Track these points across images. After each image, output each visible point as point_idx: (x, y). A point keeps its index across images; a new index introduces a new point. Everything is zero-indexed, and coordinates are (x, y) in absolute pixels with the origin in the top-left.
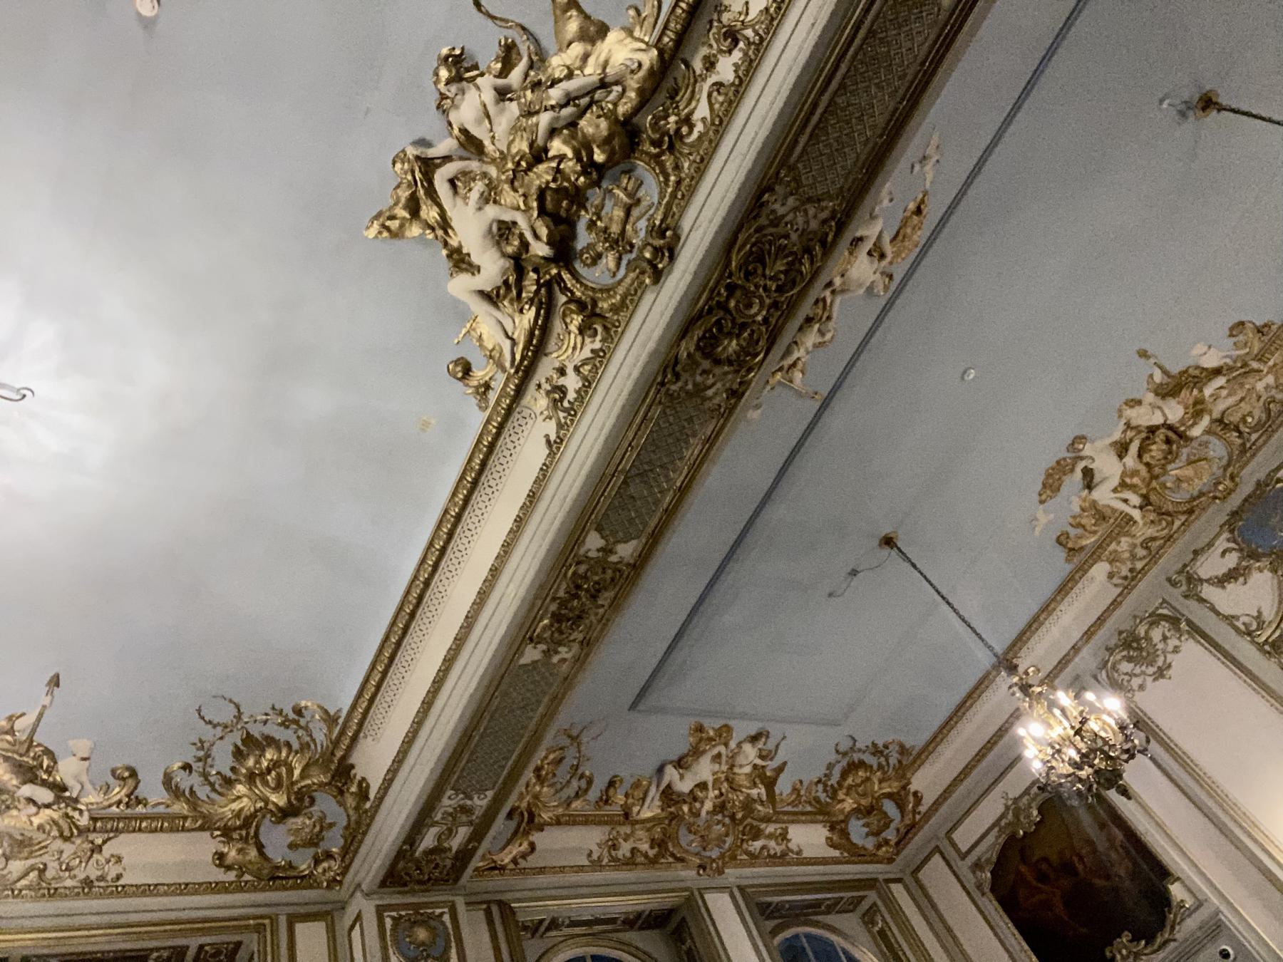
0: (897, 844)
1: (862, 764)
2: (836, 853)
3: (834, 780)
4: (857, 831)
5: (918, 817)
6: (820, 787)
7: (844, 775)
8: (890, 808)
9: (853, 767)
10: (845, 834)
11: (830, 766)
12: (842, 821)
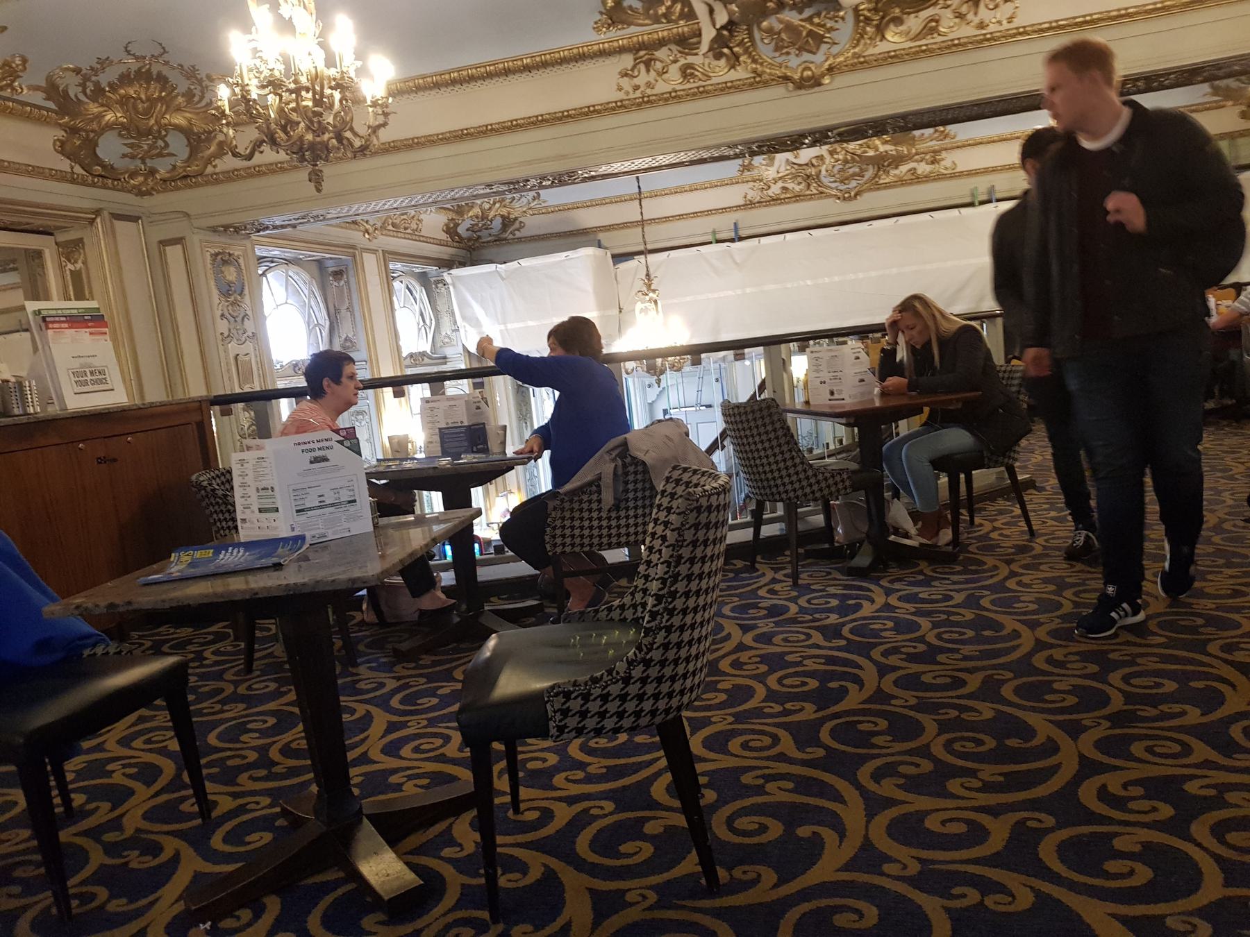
0: (165, 181)
1: (162, 79)
2: (64, 165)
3: (104, 79)
4: (111, 149)
5: (209, 169)
6: (78, 79)
7: (125, 79)
8: (178, 145)
9: (144, 76)
10: (91, 145)
11: (104, 63)
12: (93, 131)
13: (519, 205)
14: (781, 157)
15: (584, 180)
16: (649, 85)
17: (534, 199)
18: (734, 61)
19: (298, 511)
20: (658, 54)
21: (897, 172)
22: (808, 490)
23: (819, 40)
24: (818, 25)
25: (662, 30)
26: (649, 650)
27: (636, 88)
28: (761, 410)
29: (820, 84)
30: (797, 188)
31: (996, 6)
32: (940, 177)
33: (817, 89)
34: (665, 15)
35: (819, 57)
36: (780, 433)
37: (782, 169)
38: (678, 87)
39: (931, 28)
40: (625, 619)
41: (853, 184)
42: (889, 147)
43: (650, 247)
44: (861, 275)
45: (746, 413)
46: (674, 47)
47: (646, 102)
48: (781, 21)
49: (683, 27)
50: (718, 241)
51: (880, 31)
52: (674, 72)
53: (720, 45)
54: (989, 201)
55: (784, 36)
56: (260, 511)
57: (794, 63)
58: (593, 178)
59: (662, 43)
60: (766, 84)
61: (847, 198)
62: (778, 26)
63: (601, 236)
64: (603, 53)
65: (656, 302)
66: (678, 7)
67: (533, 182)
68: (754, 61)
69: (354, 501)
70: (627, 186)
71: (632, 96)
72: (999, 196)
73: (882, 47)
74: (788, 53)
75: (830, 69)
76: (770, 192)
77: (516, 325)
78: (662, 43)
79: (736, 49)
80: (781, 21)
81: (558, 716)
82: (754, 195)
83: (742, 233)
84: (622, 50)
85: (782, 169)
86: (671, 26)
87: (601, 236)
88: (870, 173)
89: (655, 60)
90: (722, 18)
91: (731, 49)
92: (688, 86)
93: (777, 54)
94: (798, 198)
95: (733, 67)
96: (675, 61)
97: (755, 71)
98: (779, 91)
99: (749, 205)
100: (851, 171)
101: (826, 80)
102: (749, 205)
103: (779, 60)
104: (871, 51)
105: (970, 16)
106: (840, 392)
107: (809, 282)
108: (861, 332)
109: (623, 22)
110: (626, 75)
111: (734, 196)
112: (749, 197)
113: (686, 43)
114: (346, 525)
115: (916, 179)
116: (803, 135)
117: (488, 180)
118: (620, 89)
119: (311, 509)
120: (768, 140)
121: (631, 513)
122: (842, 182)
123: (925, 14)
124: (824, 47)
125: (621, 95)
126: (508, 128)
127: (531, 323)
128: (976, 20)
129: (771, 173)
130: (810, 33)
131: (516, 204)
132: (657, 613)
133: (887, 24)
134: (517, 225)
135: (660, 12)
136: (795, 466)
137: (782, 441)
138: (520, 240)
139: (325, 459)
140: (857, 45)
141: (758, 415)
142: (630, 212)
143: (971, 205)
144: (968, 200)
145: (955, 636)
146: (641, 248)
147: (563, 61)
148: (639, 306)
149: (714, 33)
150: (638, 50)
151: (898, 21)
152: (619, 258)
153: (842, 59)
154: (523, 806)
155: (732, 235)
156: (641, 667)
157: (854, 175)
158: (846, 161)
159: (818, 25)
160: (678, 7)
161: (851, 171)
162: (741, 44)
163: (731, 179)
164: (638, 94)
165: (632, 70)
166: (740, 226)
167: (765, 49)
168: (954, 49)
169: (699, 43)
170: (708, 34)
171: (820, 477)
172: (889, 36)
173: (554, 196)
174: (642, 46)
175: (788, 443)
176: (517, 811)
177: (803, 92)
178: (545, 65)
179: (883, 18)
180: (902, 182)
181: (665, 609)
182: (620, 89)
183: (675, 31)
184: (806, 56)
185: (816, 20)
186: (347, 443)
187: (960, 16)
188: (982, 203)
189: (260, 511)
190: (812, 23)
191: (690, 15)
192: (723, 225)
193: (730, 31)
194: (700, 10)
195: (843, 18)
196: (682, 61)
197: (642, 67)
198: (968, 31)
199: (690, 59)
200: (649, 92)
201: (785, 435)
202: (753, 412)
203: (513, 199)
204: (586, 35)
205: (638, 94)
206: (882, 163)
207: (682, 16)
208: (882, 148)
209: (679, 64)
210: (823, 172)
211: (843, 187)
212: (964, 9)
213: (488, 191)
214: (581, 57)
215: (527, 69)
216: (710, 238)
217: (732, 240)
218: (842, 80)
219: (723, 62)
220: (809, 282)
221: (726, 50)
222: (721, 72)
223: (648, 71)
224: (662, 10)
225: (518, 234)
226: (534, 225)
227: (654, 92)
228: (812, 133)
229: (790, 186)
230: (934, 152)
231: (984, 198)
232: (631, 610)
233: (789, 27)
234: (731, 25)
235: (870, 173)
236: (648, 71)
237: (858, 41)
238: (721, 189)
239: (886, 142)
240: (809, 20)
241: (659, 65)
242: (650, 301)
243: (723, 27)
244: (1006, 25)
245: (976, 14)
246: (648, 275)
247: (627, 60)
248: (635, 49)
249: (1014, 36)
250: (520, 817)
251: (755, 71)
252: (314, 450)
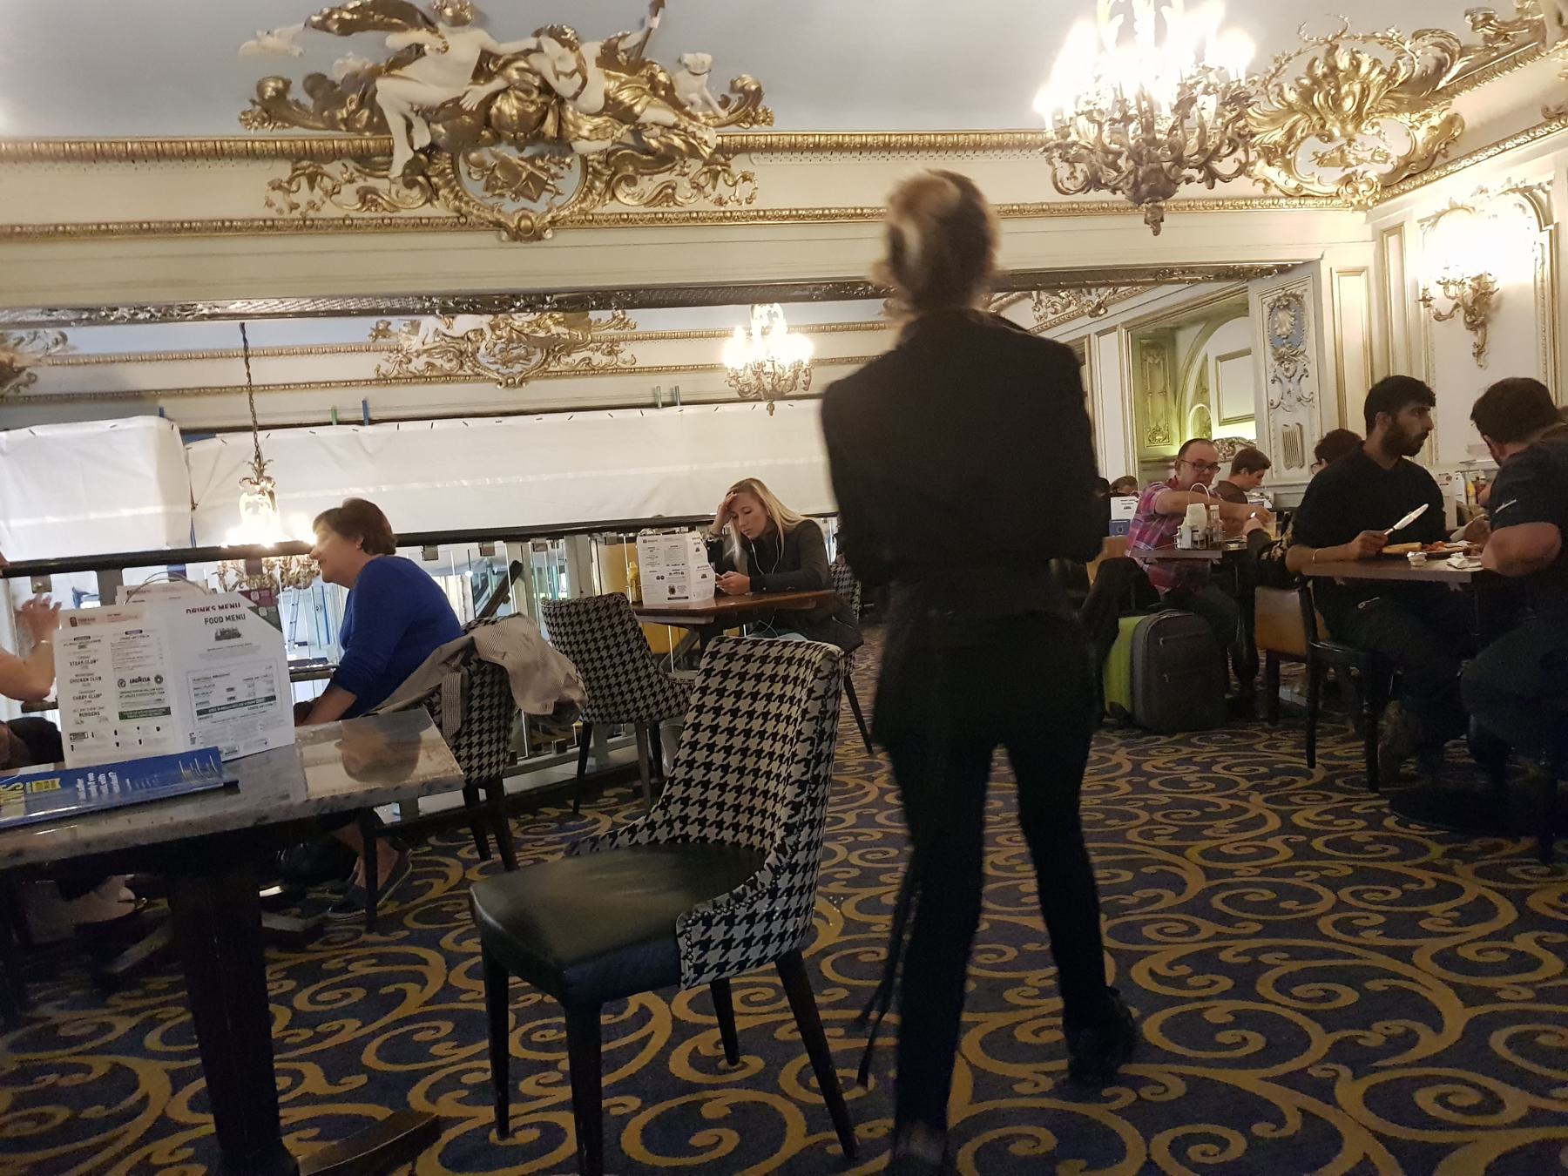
13: (29, 351)
14: (429, 323)
15: (202, 317)
16: (312, 205)
17: (57, 343)
18: (432, 193)
19: (200, 713)
20: (326, 168)
21: (569, 360)
22: (663, 706)
23: (541, 186)
24: (541, 168)
25: (340, 139)
26: (795, 852)
27: (294, 207)
28: (607, 607)
29: (540, 238)
30: (447, 366)
31: (735, 184)
32: (617, 371)
33: (535, 243)
34: (345, 121)
35: (540, 206)
36: (631, 636)
37: (429, 340)
38: (354, 215)
39: (666, 195)
40: (657, 840)
41: (518, 368)
42: (562, 330)
43: (260, 422)
44: (530, 478)
45: (578, 613)
46: (351, 164)
47: (306, 227)
48: (496, 156)
49: (369, 141)
50: (339, 423)
51: (611, 190)
52: (349, 194)
53: (416, 172)
54: (673, 404)
55: (498, 173)
56: (123, 716)
57: (510, 209)
58: (213, 317)
59: (336, 155)
60: (471, 227)
61: (511, 384)
62: (491, 162)
63: (162, 403)
64: (251, 155)
65: (271, 494)
66: (365, 113)
67: (124, 312)
68: (456, 197)
69: (274, 698)
70: (224, 335)
71: (286, 215)
72: (683, 399)
73: (611, 207)
74: (502, 196)
75: (553, 222)
76: (411, 367)
77: (25, 522)
78: (336, 155)
79: (435, 180)
80: (496, 156)
81: (696, 951)
82: (388, 368)
83: (374, 415)
84: (279, 155)
85: (429, 340)
86: (351, 135)
87: (162, 403)
88: (537, 357)
89: (323, 175)
90: (422, 138)
91: (428, 178)
92: (367, 215)
93: (488, 194)
94: (448, 377)
95: (429, 200)
96: (351, 181)
97: (458, 210)
98: (489, 238)
99: (383, 380)
100: (515, 352)
101: (548, 234)
102: (383, 380)
103: (491, 202)
104: (598, 210)
105: (708, 189)
106: (683, 588)
107: (465, 483)
108: (692, 523)
109: (284, 120)
110: (280, 187)
111: (364, 366)
112: (383, 370)
113: (369, 162)
114: (261, 735)
115: (591, 370)
116: (515, 296)
117: (52, 300)
118: (270, 204)
119: (219, 709)
120: (467, 296)
121: (475, 739)
122: (504, 364)
124: (546, 196)
125: (271, 213)
126: (134, 231)
127: (50, 519)
128: (715, 195)
129: (415, 343)
130: (531, 176)
131: (26, 348)
132: (800, 804)
133: (619, 181)
134: (24, 376)
135: (339, 116)
136: (648, 676)
137: (634, 645)
138: (29, 400)
139: (235, 634)
140: (584, 199)
141: (603, 613)
142: (234, 373)
143: (654, 406)
144: (650, 400)
145: (880, 856)
146: (250, 422)
147: (190, 155)
148: (245, 498)
149: (410, 155)
150: (300, 159)
151: (631, 180)
152: (190, 435)
153: (567, 212)
154: (512, 1124)
155: (361, 416)
156: (787, 875)
157: (519, 358)
158: (510, 340)
159: (541, 168)
160: (365, 113)
161: (515, 352)
162: (441, 174)
163: (360, 344)
164: (296, 214)
165: (290, 182)
166: (371, 405)
167: (473, 185)
168: (692, 223)
169: (391, 163)
170: (402, 155)
171: (677, 689)
172: (620, 195)
173: (87, 340)
174: (311, 155)
175: (640, 648)
176: (504, 1132)
177: (518, 244)
178: (160, 156)
179: (614, 174)
180: (574, 373)
181: (809, 798)
182: (270, 204)
183: (357, 143)
184: (524, 202)
185: (539, 162)
186: (263, 611)
187: (698, 187)
188: (665, 405)
189: (123, 716)
190: (533, 165)
191: (381, 127)
192: (350, 402)
193: (428, 156)
194: (396, 124)
195: (569, 166)
196: (360, 183)
197: (304, 182)
198: (704, 205)
199: (371, 182)
200: (312, 214)
201: (637, 639)
202: (587, 612)
203: (22, 340)
204: (229, 128)
205: (296, 214)
206: (553, 348)
207: (369, 126)
208: (555, 330)
209: (355, 186)
210: (482, 350)
211: (503, 370)
212: (702, 180)
213: (45, 318)
214: (217, 154)
215: (132, 157)
216: (329, 418)
217: (361, 423)
219: (416, 192)
220: (465, 483)
221: (420, 179)
222: (415, 205)
223: (312, 188)
224: (342, 113)
225: (24, 391)
226: (51, 379)
227: (322, 214)
228: (527, 295)
229: (438, 362)
230: (612, 341)
231: (668, 399)
232: (665, 829)
233: (505, 164)
234: (432, 149)
235: (537, 357)
236: (312, 188)
237: (585, 196)
238: (342, 356)
239: (558, 323)
240: (531, 160)
241: (327, 183)
242: (262, 492)
243: (422, 150)
244: (745, 206)
245: (714, 188)
246: (258, 456)
247: (283, 170)
248: (295, 157)
249: (754, 218)
250: (509, 1141)
251: (458, 210)
252: (220, 620)
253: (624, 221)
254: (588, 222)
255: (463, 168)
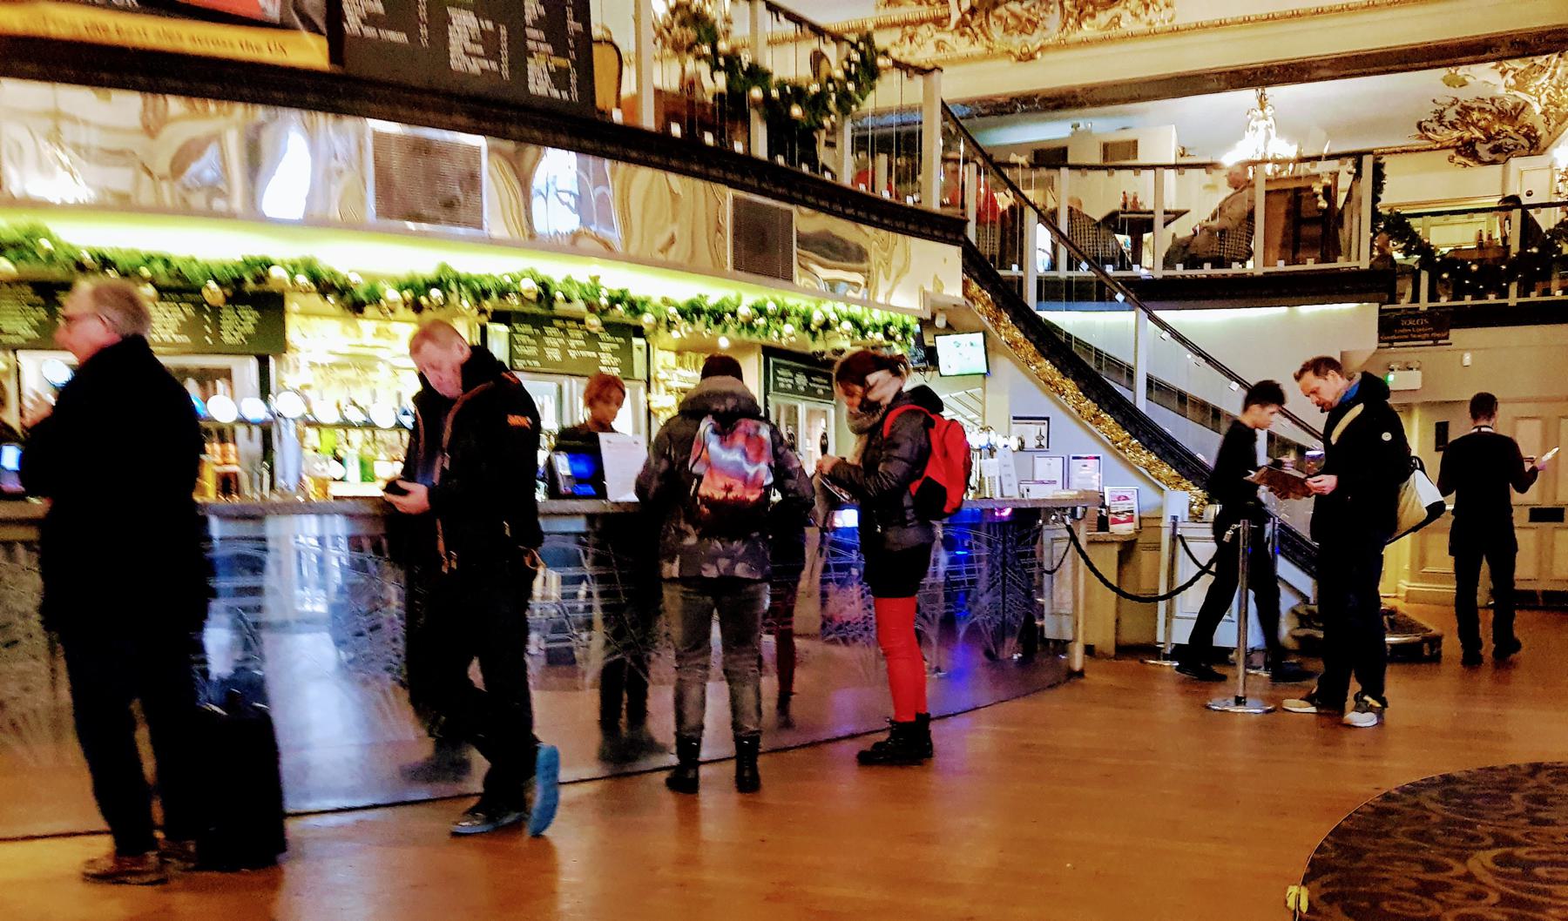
25: (924, 11)
46: (932, 26)
52: (930, 45)
53: (963, 23)
57: (1017, 42)
59: (922, 22)
73: (1078, 35)
78: (922, 22)
84: (894, 25)
101: (1039, 55)
113: (939, 22)
123: (1111, 13)
124: (1037, 32)
128: (1147, 19)
130: (1029, 20)
151: (1093, 16)
167: (996, 32)
170: (956, 16)
172: (1084, 25)
174: (905, 23)
184: (1024, 37)
187: (1136, 15)
198: (1140, 27)
218: (1051, 57)
240: (1028, 10)
253: (1087, 43)
254: (1062, 46)
255: (992, 20)
